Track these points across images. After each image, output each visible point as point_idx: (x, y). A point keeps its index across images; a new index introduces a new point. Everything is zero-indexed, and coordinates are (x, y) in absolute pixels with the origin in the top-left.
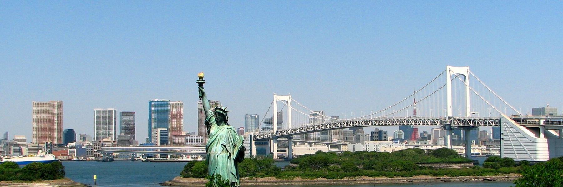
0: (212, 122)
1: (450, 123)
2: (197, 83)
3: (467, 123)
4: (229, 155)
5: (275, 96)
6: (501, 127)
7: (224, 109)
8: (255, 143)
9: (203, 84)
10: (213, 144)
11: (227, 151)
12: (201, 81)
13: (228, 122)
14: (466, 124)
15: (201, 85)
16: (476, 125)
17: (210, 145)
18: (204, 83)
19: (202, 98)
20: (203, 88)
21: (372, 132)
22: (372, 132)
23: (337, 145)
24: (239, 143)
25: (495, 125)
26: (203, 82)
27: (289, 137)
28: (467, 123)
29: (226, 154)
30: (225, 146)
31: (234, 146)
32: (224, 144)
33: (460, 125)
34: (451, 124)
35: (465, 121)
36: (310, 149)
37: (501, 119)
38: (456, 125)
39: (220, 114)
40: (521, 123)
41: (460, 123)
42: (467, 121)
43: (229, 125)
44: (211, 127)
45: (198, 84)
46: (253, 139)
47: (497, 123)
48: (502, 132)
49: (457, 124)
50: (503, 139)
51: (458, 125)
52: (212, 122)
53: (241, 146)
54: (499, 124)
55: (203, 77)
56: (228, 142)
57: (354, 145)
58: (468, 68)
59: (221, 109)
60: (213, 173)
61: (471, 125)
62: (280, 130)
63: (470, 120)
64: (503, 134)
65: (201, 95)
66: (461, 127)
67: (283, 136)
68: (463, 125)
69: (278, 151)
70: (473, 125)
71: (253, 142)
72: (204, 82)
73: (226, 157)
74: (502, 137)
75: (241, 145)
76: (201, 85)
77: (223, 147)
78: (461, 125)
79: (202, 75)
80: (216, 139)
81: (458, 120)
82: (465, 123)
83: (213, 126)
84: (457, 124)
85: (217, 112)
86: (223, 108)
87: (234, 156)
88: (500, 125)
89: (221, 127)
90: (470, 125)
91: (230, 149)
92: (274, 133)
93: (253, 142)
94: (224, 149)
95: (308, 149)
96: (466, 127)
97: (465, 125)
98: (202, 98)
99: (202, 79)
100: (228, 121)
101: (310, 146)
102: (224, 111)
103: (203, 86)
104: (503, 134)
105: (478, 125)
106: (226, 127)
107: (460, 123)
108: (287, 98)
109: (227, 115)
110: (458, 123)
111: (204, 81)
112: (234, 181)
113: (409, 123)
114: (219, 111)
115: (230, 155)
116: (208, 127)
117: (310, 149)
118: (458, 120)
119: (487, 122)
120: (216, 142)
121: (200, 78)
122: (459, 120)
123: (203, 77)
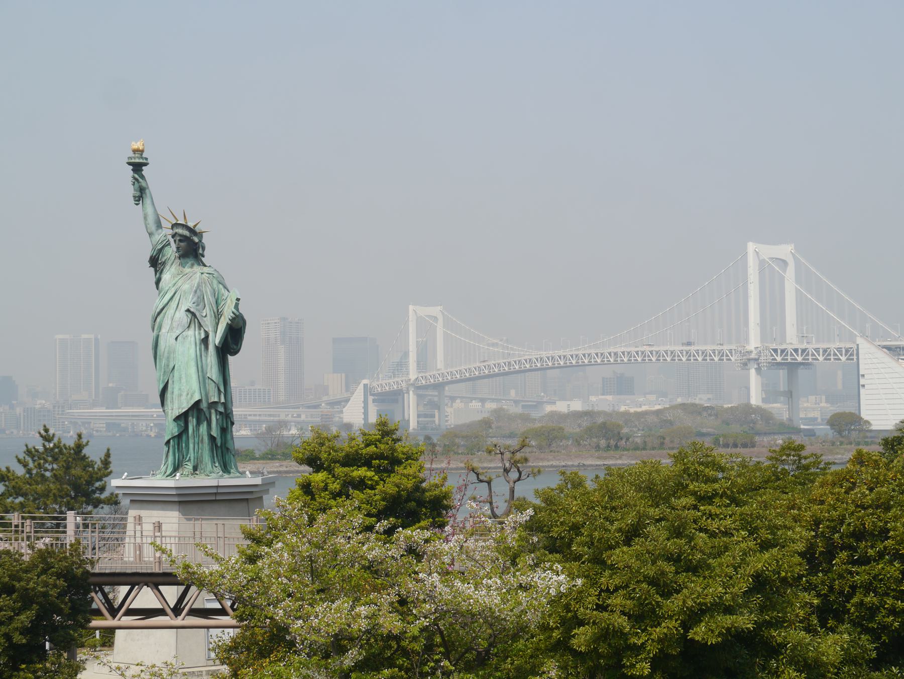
0: (165, 258)
1: (757, 357)
2: (129, 164)
3: (792, 355)
4: (203, 336)
5: (411, 307)
6: (860, 363)
7: (195, 226)
8: (374, 401)
9: (144, 168)
10: (164, 311)
11: (200, 326)
12: (137, 160)
13: (203, 259)
14: (789, 357)
15: (137, 167)
16: (808, 359)
17: (159, 314)
18: (146, 164)
19: (141, 202)
20: (143, 177)
21: (603, 378)
22: (603, 378)
23: (535, 403)
24: (229, 307)
25: (847, 359)
26: (141, 161)
27: (439, 387)
28: (792, 355)
29: (197, 332)
30: (193, 314)
31: (218, 316)
32: (192, 310)
33: (775, 359)
34: (758, 359)
35: (787, 352)
36: (482, 412)
37: (860, 347)
38: (770, 361)
39: (184, 239)
40: (899, 355)
41: (777, 355)
42: (791, 352)
43: (205, 266)
44: (162, 270)
45: (131, 167)
46: (370, 392)
47: (850, 355)
48: (861, 373)
49: (771, 358)
50: (863, 386)
51: (773, 359)
52: (165, 258)
53: (232, 315)
54: (855, 357)
55: (142, 151)
56: (202, 305)
57: (569, 403)
58: (793, 245)
59: (185, 227)
60: (166, 381)
61: (799, 359)
62: (420, 375)
63: (796, 350)
64: (863, 376)
65: (138, 194)
66: (779, 364)
67: (429, 386)
68: (783, 359)
69: (419, 416)
71: (371, 398)
72: (145, 161)
73: (198, 342)
74: (862, 382)
75: (233, 313)
76: (137, 167)
77: (190, 315)
78: (779, 359)
79: (138, 145)
80: (174, 299)
81: (773, 350)
83: (167, 267)
84: (771, 358)
85: (176, 233)
86: (191, 224)
87: (216, 339)
88: (858, 359)
89: (187, 270)
90: (797, 360)
91: (208, 324)
92: (410, 380)
94: (193, 322)
95: (478, 412)
96: (789, 362)
97: (787, 359)
98: (141, 202)
99: (142, 154)
100: (203, 256)
101: (483, 406)
102: (192, 231)
103: (143, 172)
104: (863, 376)
105: (813, 359)
106: (197, 269)
108: (436, 311)
109: (200, 241)
110: (772, 355)
111: (146, 159)
112: (216, 400)
113: (676, 358)
114: (180, 231)
115: (207, 337)
116: (156, 272)
117: (482, 412)
118: (773, 350)
119: (832, 353)
120: (173, 304)
121: (135, 151)
122: (775, 351)
123: (142, 151)
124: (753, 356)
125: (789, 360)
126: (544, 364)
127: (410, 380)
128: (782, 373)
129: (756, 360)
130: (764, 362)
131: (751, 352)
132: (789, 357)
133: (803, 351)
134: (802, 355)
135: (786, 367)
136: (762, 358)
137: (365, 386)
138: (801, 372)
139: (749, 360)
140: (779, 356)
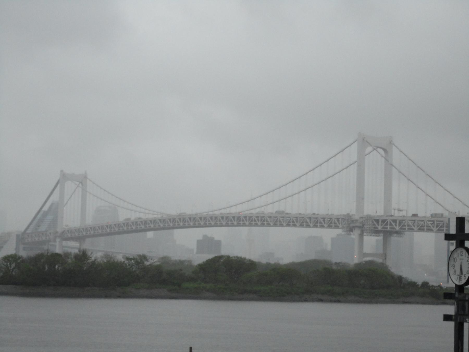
1: (361, 225)
3: (391, 224)
14: (389, 227)
28: (391, 224)
33: (377, 228)
35: (387, 222)
41: (378, 225)
42: (390, 223)
49: (374, 226)
51: (374, 228)
61: (397, 228)
68: (382, 228)
70: (401, 228)
78: (380, 228)
82: (387, 224)
84: (374, 226)
90: (395, 229)
93: (21, 247)
97: (387, 228)
107: (378, 225)
122: (377, 221)
124: (358, 224)
125: (388, 229)
126: (176, 224)
127: (57, 232)
128: (381, 238)
129: (360, 227)
130: (367, 230)
131: (357, 220)
132: (389, 227)
133: (401, 222)
134: (399, 226)
135: (382, 234)
136: (366, 226)
137: (18, 236)
138: (394, 239)
139: (354, 227)
140: (380, 225)
